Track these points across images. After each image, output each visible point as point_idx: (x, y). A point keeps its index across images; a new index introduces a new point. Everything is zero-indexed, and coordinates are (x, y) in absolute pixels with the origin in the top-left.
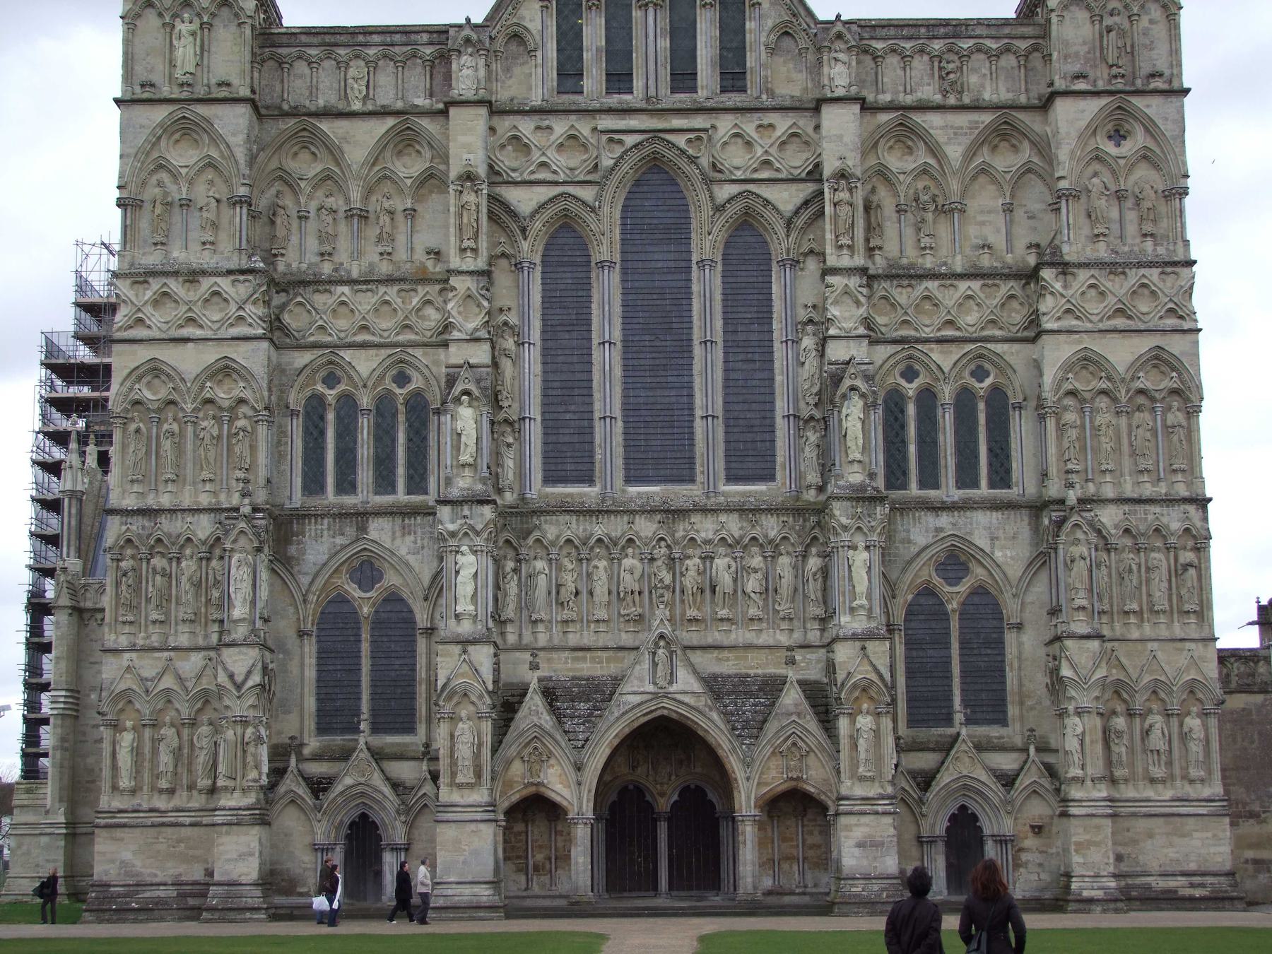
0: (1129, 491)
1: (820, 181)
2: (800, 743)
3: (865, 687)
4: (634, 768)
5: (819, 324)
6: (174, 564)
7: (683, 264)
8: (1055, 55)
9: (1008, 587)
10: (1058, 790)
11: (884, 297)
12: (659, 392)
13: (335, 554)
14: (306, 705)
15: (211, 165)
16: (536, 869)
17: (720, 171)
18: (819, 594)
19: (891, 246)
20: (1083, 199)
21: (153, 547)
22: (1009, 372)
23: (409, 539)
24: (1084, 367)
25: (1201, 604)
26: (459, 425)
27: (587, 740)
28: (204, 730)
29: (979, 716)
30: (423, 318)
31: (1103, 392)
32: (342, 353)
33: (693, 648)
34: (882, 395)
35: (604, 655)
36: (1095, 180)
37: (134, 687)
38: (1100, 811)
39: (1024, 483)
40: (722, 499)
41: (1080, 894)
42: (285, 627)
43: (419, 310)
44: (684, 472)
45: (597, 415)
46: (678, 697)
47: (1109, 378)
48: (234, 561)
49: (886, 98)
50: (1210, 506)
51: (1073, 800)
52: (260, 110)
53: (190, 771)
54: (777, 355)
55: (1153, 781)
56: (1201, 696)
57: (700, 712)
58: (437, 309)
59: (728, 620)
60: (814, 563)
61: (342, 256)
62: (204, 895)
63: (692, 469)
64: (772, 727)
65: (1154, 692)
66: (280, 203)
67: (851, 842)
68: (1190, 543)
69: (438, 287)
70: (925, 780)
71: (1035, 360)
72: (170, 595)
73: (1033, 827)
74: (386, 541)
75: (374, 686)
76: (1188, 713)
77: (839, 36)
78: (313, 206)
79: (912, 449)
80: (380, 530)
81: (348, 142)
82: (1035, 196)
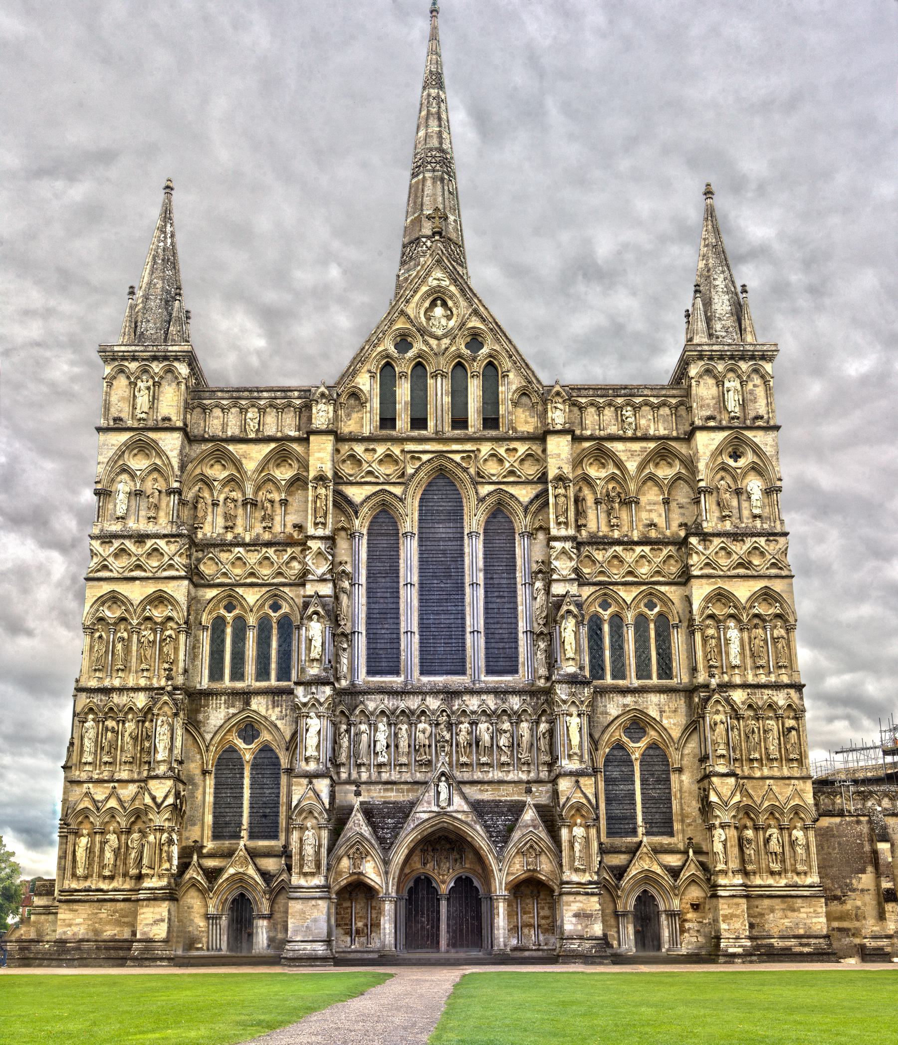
0: (751, 679)
1: (546, 483)
2: (536, 846)
3: (578, 808)
4: (425, 864)
5: (546, 572)
6: (121, 725)
7: (459, 535)
8: (695, 405)
10: (709, 880)
11: (587, 556)
12: (443, 616)
13: (229, 719)
14: (206, 820)
15: (156, 469)
17: (483, 477)
18: (547, 747)
19: (592, 526)
20: (715, 494)
21: (107, 713)
22: (670, 604)
23: (277, 710)
24: (719, 600)
25: (800, 754)
26: (311, 634)
27: (392, 843)
28: (136, 836)
29: (655, 830)
30: (291, 568)
31: (732, 616)
32: (237, 590)
33: (464, 783)
34: (587, 618)
35: (405, 787)
36: (722, 482)
37: (90, 807)
38: (739, 893)
39: (681, 676)
40: (483, 685)
41: (726, 951)
42: (194, 768)
43: (288, 563)
44: (459, 668)
45: (402, 630)
46: (454, 814)
47: (735, 607)
48: (159, 723)
49: (588, 433)
50: (804, 690)
51: (721, 886)
52: (190, 439)
53: (125, 864)
54: (519, 592)
55: (772, 873)
56: (803, 816)
58: (299, 562)
59: (487, 764)
60: (543, 727)
61: (239, 530)
62: (129, 949)
63: (464, 666)
64: (516, 835)
65: (772, 813)
66: (201, 495)
67: (571, 914)
68: (792, 714)
69: (300, 548)
70: (620, 872)
71: (687, 596)
72: (117, 745)
73: (692, 905)
74: (263, 712)
75: (251, 807)
76: (795, 828)
77: (558, 394)
78: (222, 498)
79: (607, 653)
80: (259, 704)
81: (245, 458)
82: (682, 495)
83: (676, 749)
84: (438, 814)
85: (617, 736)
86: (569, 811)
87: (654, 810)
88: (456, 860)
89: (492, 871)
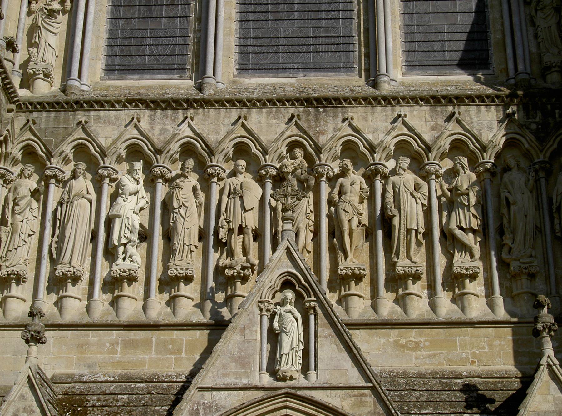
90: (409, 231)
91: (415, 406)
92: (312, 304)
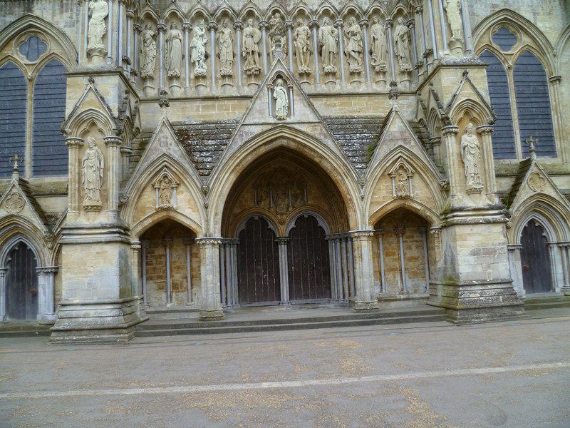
3: (468, 109)
4: (259, 202)
9: (550, 50)
16: (175, 286)
23: (66, 15)
35: (230, 103)
46: (297, 127)
57: (316, 139)
59: (334, 74)
64: (381, 151)
70: (508, 199)
74: (48, 18)
83: (555, 55)
84: (275, 126)
85: (486, 41)
86: (457, 113)
87: (533, 127)
88: (296, 196)
89: (351, 200)
90: (330, 52)
91: (335, 131)
92: (291, 85)
